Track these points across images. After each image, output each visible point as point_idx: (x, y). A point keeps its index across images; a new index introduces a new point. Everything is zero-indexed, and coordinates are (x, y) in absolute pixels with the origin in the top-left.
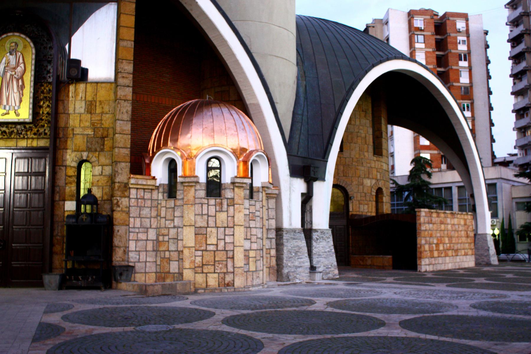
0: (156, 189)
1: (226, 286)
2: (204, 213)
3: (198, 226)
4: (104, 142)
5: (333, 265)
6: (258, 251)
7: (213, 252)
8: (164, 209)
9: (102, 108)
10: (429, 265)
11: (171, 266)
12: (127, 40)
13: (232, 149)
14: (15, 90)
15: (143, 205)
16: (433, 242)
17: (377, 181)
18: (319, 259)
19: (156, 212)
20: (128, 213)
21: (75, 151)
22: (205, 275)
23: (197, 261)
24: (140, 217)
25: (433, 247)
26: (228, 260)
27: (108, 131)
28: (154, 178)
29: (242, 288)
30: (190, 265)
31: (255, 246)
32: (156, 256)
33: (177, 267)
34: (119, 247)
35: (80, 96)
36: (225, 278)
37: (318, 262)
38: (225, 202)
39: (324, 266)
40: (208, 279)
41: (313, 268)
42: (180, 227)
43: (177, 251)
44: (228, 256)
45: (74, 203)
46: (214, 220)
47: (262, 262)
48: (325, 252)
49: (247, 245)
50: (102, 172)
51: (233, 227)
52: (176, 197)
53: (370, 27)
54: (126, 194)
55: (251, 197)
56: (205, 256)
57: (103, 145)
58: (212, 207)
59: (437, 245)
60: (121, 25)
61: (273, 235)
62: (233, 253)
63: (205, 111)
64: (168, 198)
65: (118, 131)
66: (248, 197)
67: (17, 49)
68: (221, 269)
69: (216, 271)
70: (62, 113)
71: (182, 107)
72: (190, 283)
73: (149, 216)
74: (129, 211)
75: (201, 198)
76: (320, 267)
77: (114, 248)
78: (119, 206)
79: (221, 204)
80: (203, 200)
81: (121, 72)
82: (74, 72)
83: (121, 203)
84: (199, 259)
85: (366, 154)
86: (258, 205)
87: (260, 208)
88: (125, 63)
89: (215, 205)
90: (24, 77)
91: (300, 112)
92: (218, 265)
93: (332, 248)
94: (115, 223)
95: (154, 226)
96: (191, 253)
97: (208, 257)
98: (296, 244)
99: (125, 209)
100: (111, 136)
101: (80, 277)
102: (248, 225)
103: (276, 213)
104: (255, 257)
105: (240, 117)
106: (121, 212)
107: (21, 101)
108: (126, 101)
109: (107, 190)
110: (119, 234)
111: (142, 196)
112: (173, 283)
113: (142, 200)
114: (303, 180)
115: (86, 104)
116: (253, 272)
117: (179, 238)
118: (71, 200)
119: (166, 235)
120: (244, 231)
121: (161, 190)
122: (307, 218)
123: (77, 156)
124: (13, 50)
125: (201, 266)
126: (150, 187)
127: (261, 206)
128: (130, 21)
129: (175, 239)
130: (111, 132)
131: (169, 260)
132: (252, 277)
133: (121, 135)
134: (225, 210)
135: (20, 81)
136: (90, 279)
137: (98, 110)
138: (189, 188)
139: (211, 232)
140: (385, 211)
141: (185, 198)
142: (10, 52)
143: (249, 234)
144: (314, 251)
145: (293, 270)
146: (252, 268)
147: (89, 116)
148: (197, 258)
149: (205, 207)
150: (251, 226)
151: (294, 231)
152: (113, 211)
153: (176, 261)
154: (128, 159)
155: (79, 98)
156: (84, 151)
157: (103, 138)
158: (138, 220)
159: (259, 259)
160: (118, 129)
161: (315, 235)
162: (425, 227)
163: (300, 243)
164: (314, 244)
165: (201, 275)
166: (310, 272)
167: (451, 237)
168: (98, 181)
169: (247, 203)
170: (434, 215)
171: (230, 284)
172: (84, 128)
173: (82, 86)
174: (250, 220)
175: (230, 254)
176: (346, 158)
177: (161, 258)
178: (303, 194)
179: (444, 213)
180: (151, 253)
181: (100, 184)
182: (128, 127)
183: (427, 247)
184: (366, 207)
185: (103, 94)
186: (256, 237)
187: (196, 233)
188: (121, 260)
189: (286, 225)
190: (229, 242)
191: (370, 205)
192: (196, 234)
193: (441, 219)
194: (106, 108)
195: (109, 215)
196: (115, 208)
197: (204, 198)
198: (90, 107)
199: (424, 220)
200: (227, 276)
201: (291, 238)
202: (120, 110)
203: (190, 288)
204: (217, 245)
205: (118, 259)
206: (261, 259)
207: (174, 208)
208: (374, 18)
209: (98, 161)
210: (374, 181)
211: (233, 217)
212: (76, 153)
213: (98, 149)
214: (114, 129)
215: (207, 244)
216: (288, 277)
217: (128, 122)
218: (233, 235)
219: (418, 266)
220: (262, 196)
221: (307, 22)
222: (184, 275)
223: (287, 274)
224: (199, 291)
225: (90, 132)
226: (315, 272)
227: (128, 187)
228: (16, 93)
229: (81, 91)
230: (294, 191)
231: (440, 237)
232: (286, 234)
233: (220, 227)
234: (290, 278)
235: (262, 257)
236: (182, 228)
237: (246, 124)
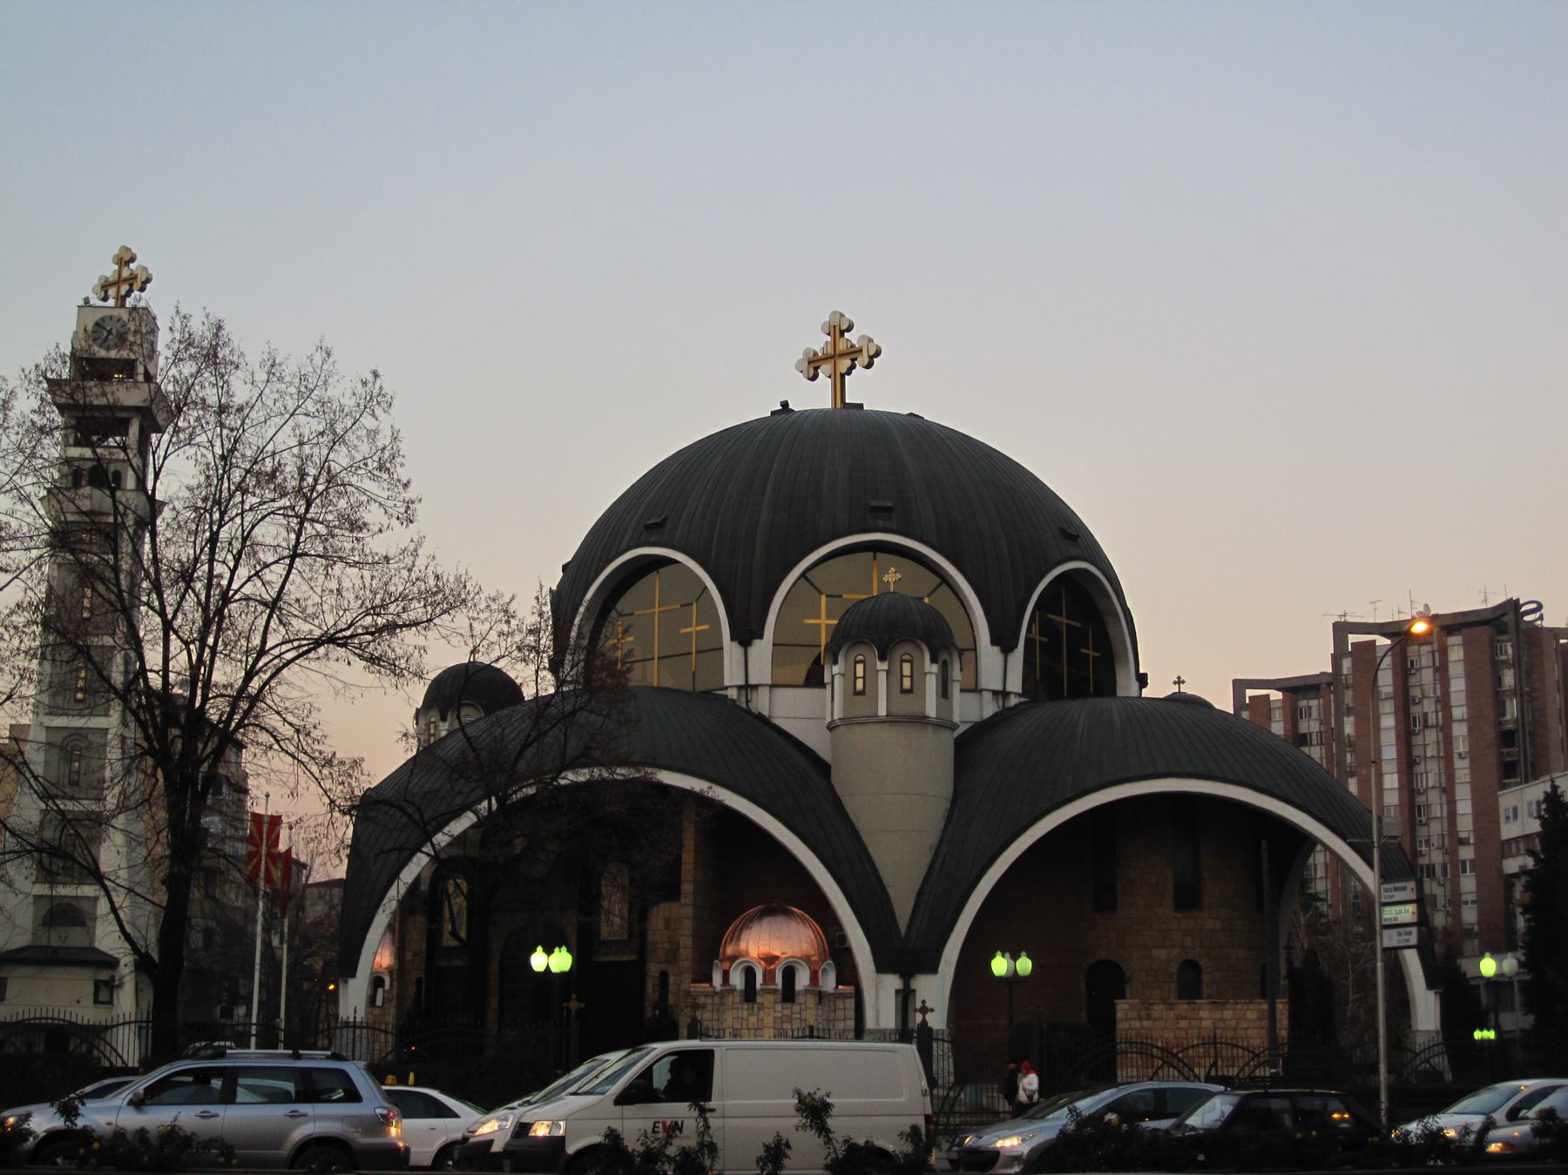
38: (756, 1006)
79: (753, 1009)
86: (796, 1008)
137: (672, 928)
169: (779, 1007)
178: (897, 992)
193: (1177, 1012)
210: (1176, 951)
225: (667, 946)
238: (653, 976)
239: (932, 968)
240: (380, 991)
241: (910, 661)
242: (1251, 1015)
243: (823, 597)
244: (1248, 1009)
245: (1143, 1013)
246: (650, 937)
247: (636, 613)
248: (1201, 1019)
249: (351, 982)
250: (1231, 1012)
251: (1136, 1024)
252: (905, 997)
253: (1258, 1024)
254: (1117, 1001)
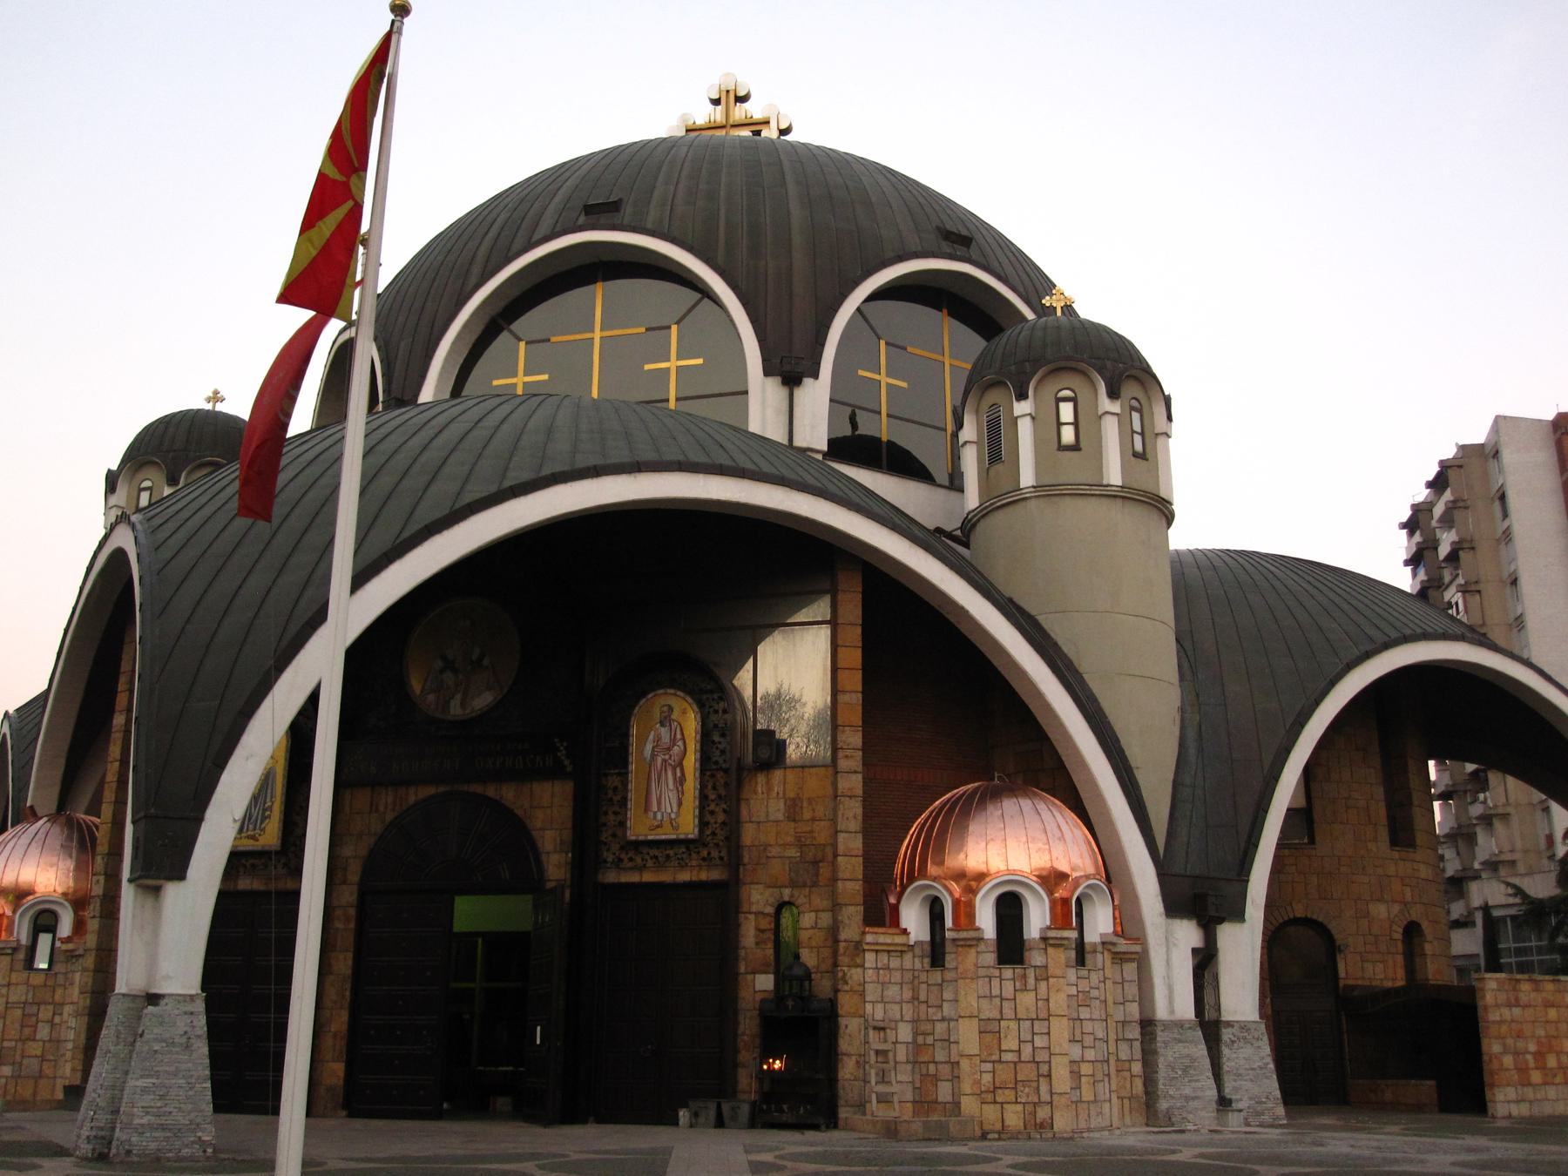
0: (908, 951)
1: (1038, 1127)
2: (994, 994)
3: (983, 1017)
4: (818, 871)
5: (1271, 1097)
6: (1099, 1065)
7: (1012, 1065)
8: (924, 986)
9: (813, 810)
10: (1518, 1102)
11: (939, 1089)
12: (850, 692)
13: (1038, 876)
14: (671, 786)
15: (887, 980)
16: (1526, 1048)
17: (1405, 905)
18: (1239, 1083)
19: (911, 994)
20: (862, 994)
21: (770, 887)
22: (998, 1106)
23: (983, 1082)
24: (882, 1001)
25: (1526, 1062)
26: (1041, 1079)
27: (824, 850)
28: (905, 932)
29: (1066, 1132)
30: (972, 1089)
31: (1090, 1054)
32: (913, 1071)
33: (951, 1091)
34: (849, 1055)
35: (776, 791)
36: (1035, 1112)
37: (1236, 1089)
38: (1031, 974)
39: (1251, 1099)
40: (1005, 1115)
41: (1224, 1103)
42: (953, 1020)
43: (949, 1062)
44: (1041, 1072)
45: (771, 977)
46: (1013, 1007)
47: (1107, 1085)
48: (1253, 1069)
49: (1075, 1052)
50: (816, 923)
51: (1048, 1020)
52: (944, 966)
53: (1450, 467)
54: (858, 961)
55: (1081, 960)
56: (998, 1072)
57: (817, 874)
58: (1008, 983)
59: (1540, 1056)
60: (839, 666)
61: (1134, 1032)
62: (1050, 1066)
63: (990, 808)
64: (931, 967)
65: (840, 851)
66: (1074, 964)
67: (672, 717)
68: (1028, 1097)
69: (1019, 1100)
70: (746, 822)
71: (949, 800)
72: (974, 1121)
73: (898, 999)
74: (864, 991)
75: (988, 967)
76: (1241, 1100)
77: (840, 1057)
78: (847, 984)
79: (1024, 976)
80: (992, 970)
81: (841, 748)
82: (764, 753)
83: (851, 977)
84: (987, 1078)
85: (1371, 846)
86: (1095, 977)
87: (1100, 982)
88: (848, 732)
89: (1014, 979)
90: (685, 763)
91: (1188, 780)
92: (1022, 1089)
93: (1269, 1060)
94: (840, 1012)
95: (908, 1016)
96: (973, 1066)
97: (1005, 1074)
98: (1186, 1051)
99: (857, 988)
100: (830, 857)
101: (785, 1107)
102: (1075, 1015)
103: (1140, 989)
104: (1093, 1075)
105: (1054, 816)
106: (850, 993)
107: (680, 804)
108: (853, 799)
109: (826, 952)
110: (848, 1031)
111: (884, 965)
112: (943, 1119)
113: (887, 972)
114: (1195, 922)
115: (785, 804)
116: (1088, 1102)
117: (952, 1040)
118: (766, 972)
119: (928, 1034)
120: (1069, 1025)
121: (917, 951)
122: (1208, 998)
123: (775, 895)
124: (665, 718)
125: (992, 1089)
126: (899, 948)
127: (1102, 979)
128: (853, 657)
129: (945, 1040)
130: (829, 850)
131: (936, 1079)
132: (1087, 1112)
133: (847, 858)
134: (1033, 987)
135: (678, 770)
136: (802, 1111)
137: (807, 815)
138: (967, 949)
139: (1008, 1027)
140: (1430, 977)
141: (960, 967)
142: (661, 722)
143: (1078, 1032)
144: (1227, 1065)
145: (1179, 1104)
146: (1087, 1095)
147: (792, 824)
148: (984, 1075)
149: (996, 982)
150: (1082, 1017)
151: (1180, 1025)
152: (836, 991)
153: (948, 1080)
154: (860, 899)
155: (775, 795)
156: (786, 887)
157: (816, 863)
158: (879, 1007)
159: (1101, 1079)
160: (841, 848)
161: (1226, 1035)
163: (1195, 1050)
164: (1225, 1051)
165: (992, 1106)
166: (1218, 1110)
168: (810, 938)
169: (1072, 974)
170: (1525, 987)
171: (1045, 1124)
172: (785, 845)
173: (778, 774)
174: (1079, 1006)
175: (1044, 1069)
176: (1322, 857)
177: (921, 1075)
179: (1553, 981)
180: (904, 1066)
181: (814, 944)
182: (857, 843)
183: (1508, 1061)
184: (1380, 966)
185: (815, 784)
186: (1092, 1037)
187: (982, 1029)
188: (852, 1078)
189: (1161, 1013)
190: (1040, 1046)
191: (1391, 962)
192: (980, 1032)
193: (1544, 995)
194: (820, 811)
195: (830, 999)
196: (840, 987)
197: (993, 967)
198: (792, 810)
199: (1496, 998)
200: (1039, 1110)
201: (1175, 1039)
202: (843, 815)
203: (974, 1131)
204: (1019, 1051)
205: (847, 1076)
206: (1106, 1079)
207: (941, 985)
208: (1461, 443)
209: (810, 903)
210: (1396, 908)
211: (1048, 1000)
212: (771, 890)
213: (809, 884)
214: (835, 846)
215: (1001, 1051)
216: (1170, 1118)
217: (857, 835)
218: (1049, 1033)
219: (1489, 1104)
220: (1101, 960)
221: (1218, 563)
222: (963, 1107)
223: (1167, 1113)
224: (990, 1136)
225: (793, 853)
226: (1228, 1111)
227: (861, 948)
228: (672, 790)
229: (777, 782)
230: (1175, 945)
231: (1546, 1037)
232: (1162, 1031)
233: (1022, 1019)
234: (1173, 1119)
235: (1109, 1075)
236: (957, 1020)
237: (1064, 827)
238: (757, 914)
239: (1237, 913)
240: (45, 940)
241: (1140, 411)
243: (882, 343)
246: (749, 835)
247: (554, 339)
249: (172, 891)
251: (1506, 1013)
252: (1205, 962)
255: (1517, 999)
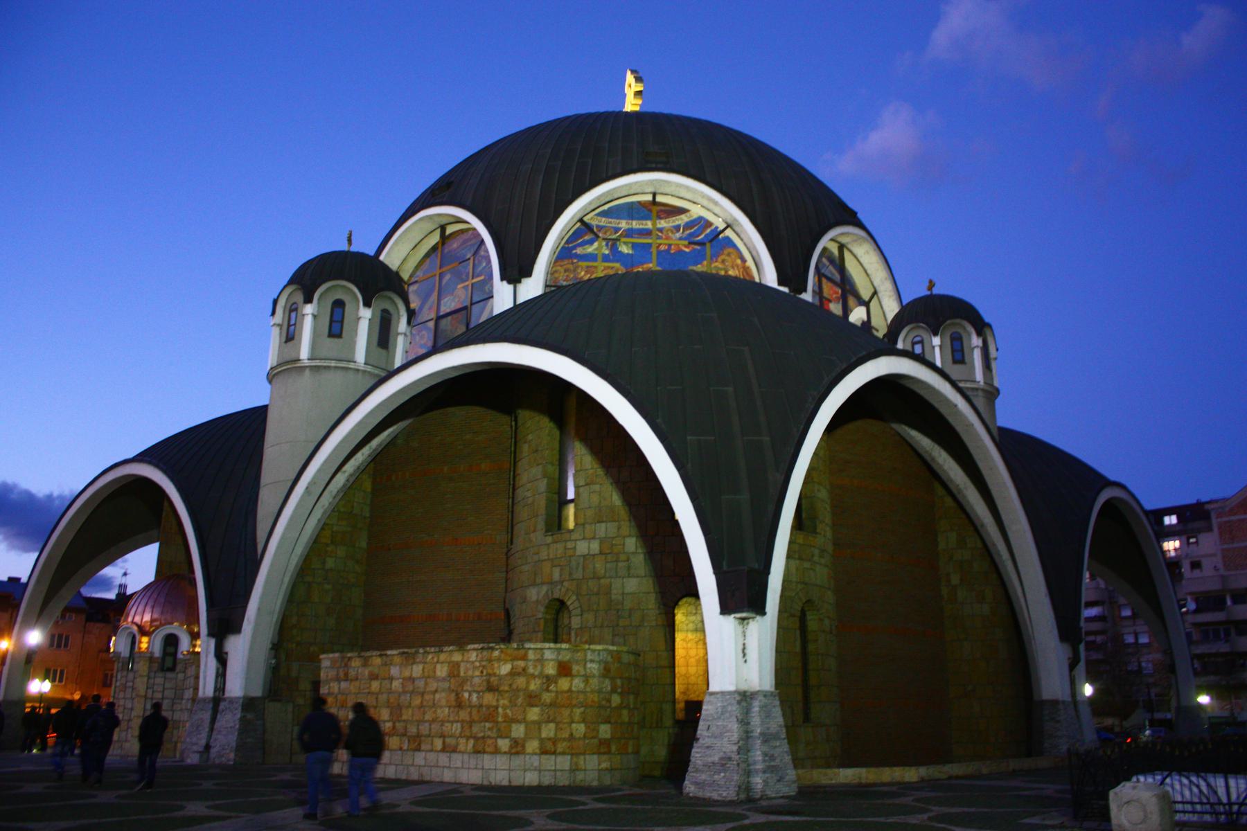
48: (227, 728)
86: (131, 676)
162: (327, 687)
164: (219, 716)
167: (400, 707)
170: (356, 663)
179: (381, 655)
193: (370, 669)
199: (327, 676)
210: (545, 588)
242: (442, 671)
244: (438, 662)
245: (342, 674)
248: (391, 679)
250: (421, 667)
251: (335, 687)
253: (446, 685)
254: (322, 656)
255: (346, 674)
